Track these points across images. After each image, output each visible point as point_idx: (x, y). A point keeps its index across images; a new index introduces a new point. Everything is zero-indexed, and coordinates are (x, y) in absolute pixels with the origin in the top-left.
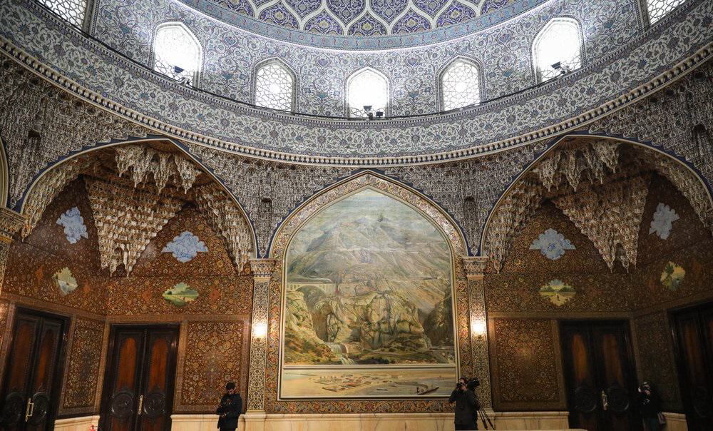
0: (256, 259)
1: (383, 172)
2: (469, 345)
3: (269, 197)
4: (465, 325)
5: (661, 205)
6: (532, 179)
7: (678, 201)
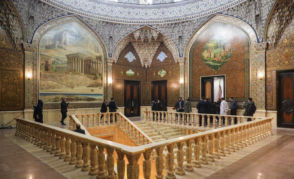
0: (26, 43)
1: (82, 18)
2: (107, 86)
3: (32, 15)
4: (106, 80)
5: (162, 53)
6: (132, 35)
7: (167, 51)
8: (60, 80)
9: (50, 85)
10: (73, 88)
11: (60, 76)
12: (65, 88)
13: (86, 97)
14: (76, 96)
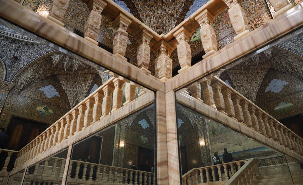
8: (226, 140)
9: (219, 148)
10: (241, 144)
11: (225, 136)
12: (233, 146)
13: (261, 151)
14: (247, 152)
